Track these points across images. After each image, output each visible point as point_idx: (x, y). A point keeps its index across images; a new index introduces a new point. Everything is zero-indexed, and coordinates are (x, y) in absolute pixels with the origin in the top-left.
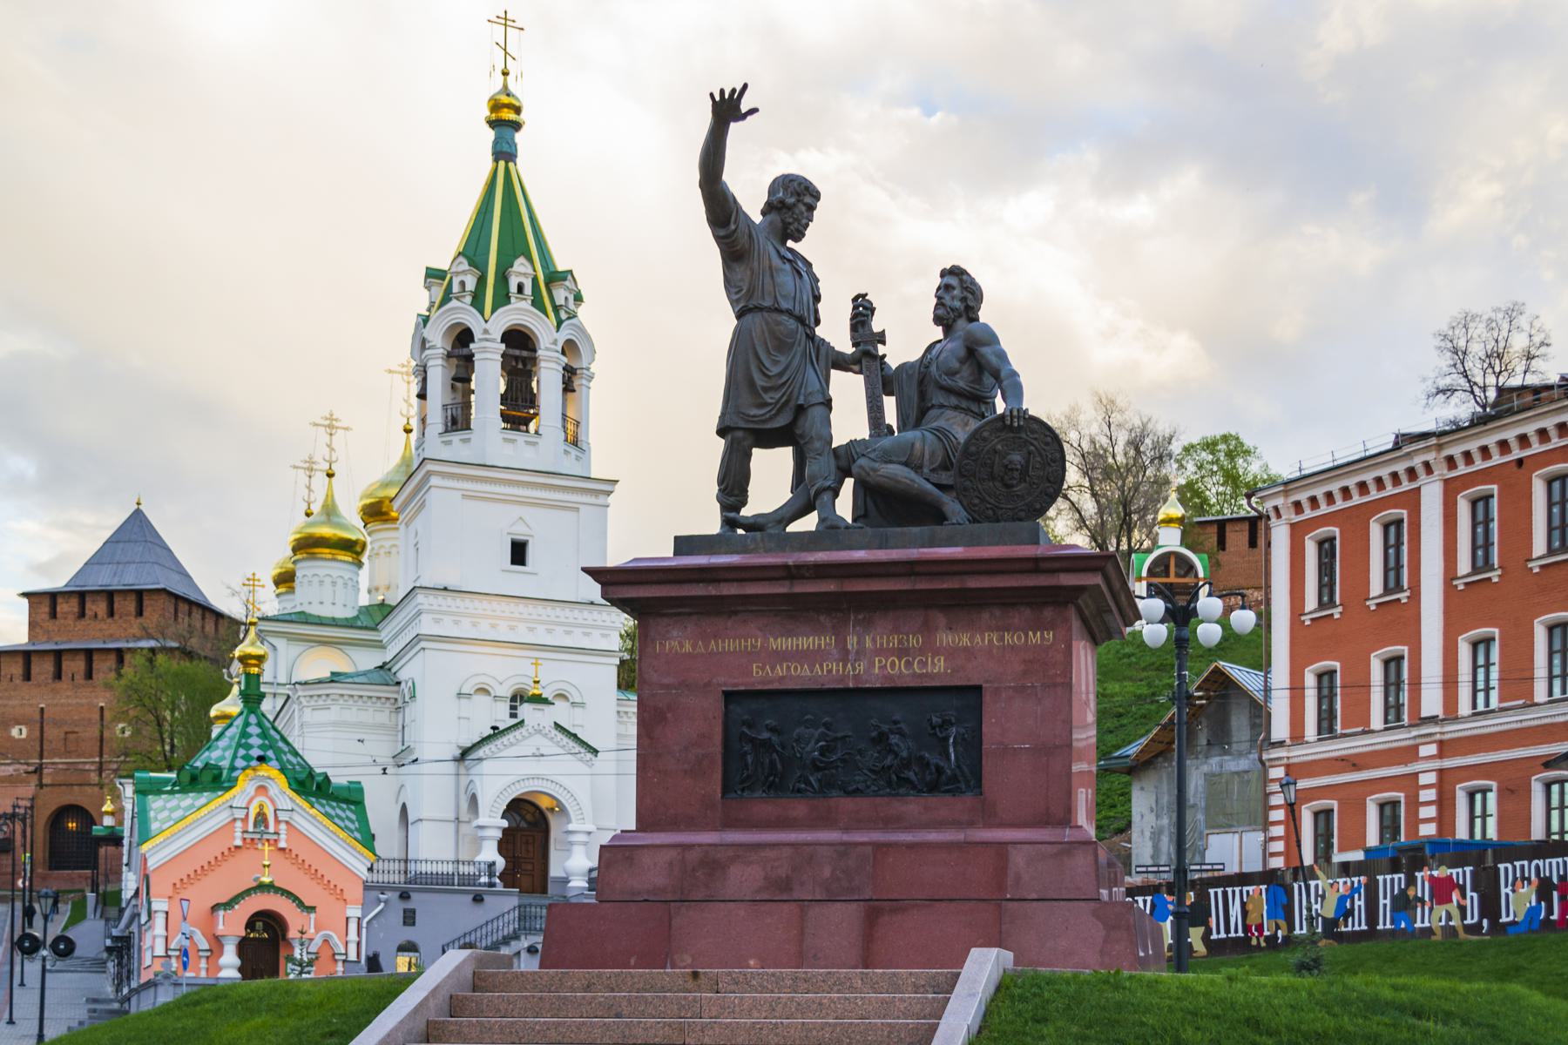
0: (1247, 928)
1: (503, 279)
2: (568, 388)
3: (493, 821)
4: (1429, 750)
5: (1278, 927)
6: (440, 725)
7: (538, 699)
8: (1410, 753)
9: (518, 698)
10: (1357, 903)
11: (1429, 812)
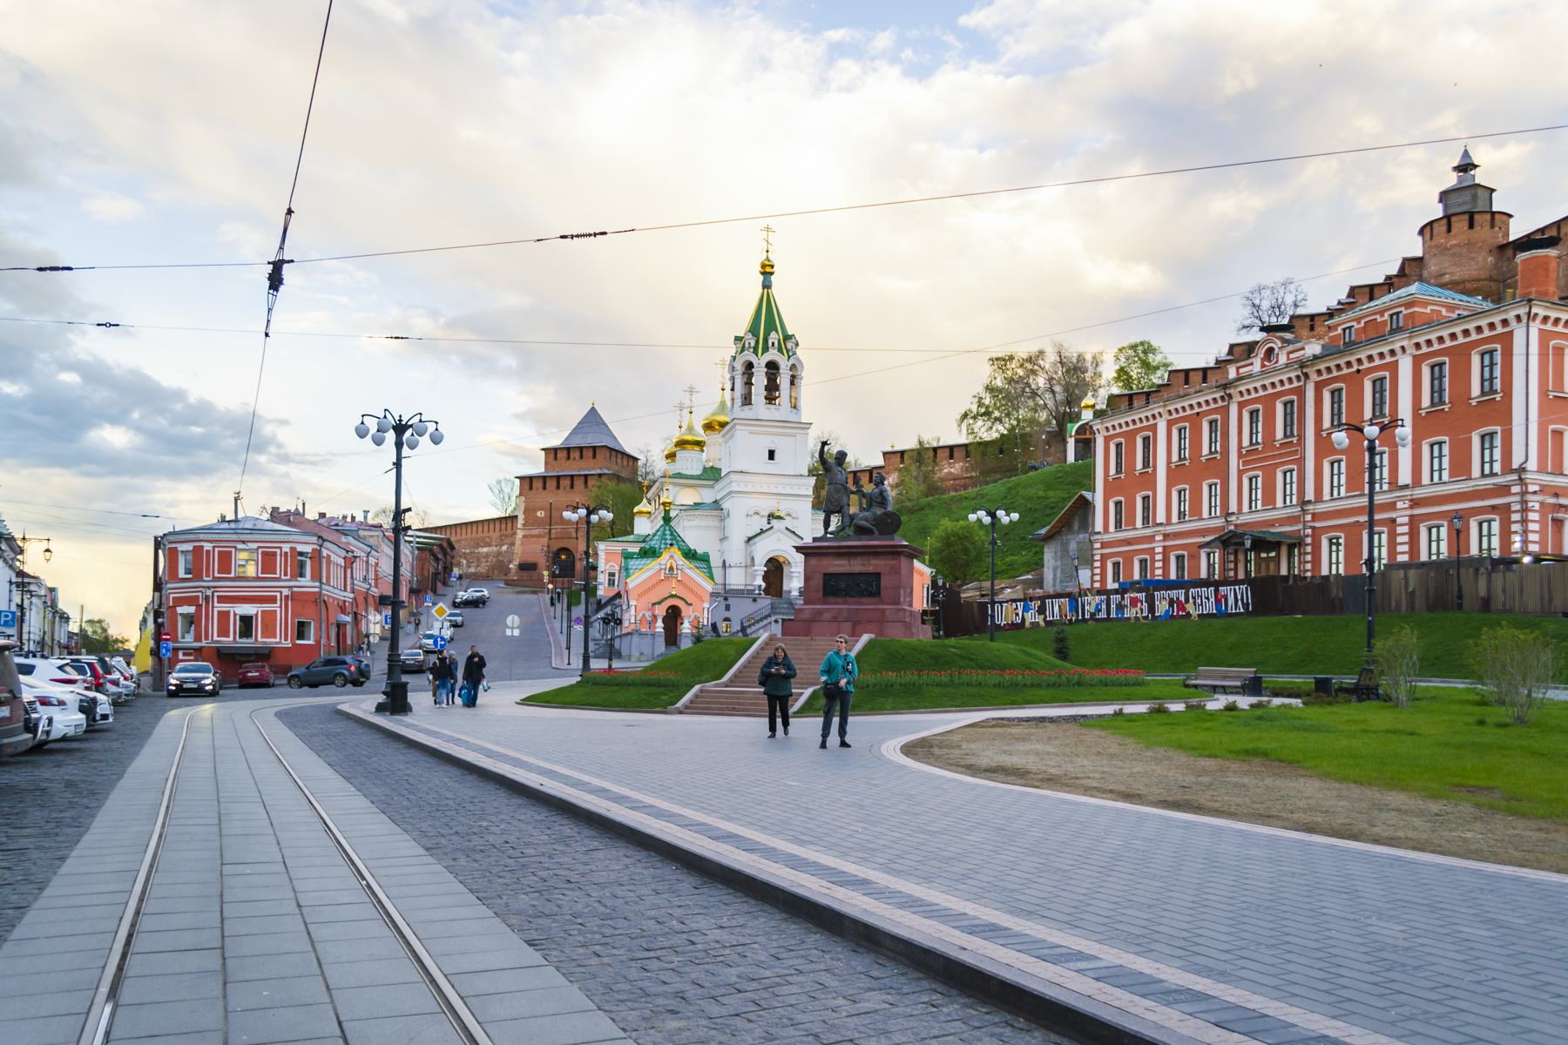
1: (766, 341)
2: (792, 383)
3: (761, 569)
4: (1159, 538)
6: (739, 528)
7: (780, 518)
8: (1151, 539)
9: (771, 516)
11: (1159, 564)
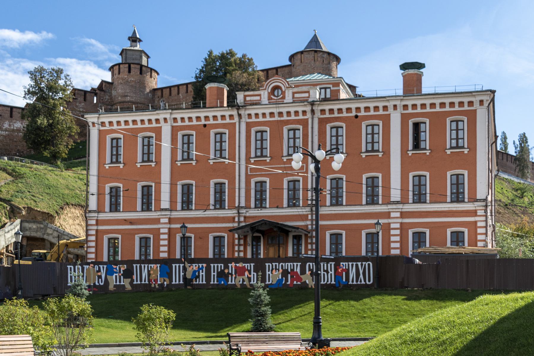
0: (149, 280)
5: (164, 281)
10: (201, 274)
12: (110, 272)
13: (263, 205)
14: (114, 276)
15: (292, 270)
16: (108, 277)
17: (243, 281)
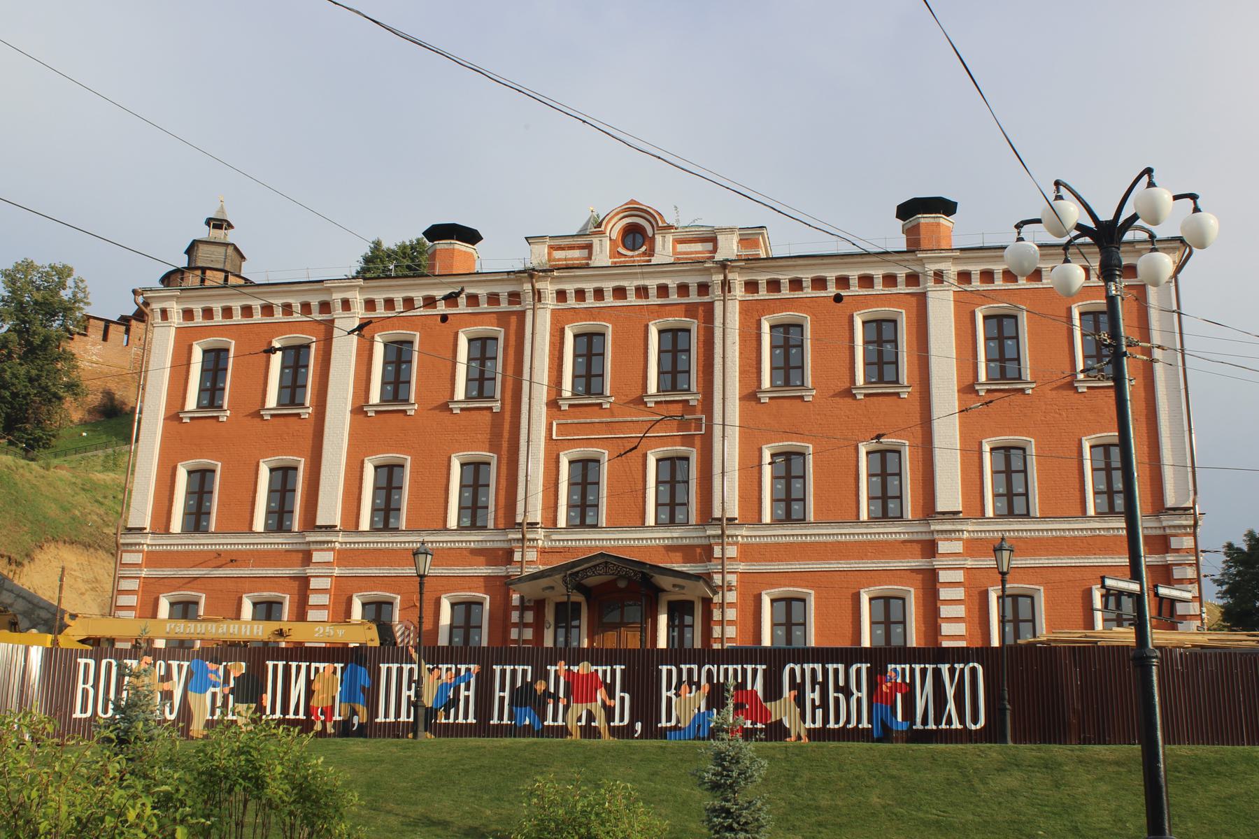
5: (354, 712)
10: (463, 693)
12: (194, 682)
13: (588, 521)
14: (208, 695)
15: (741, 687)
16: (192, 696)
17: (591, 718)
